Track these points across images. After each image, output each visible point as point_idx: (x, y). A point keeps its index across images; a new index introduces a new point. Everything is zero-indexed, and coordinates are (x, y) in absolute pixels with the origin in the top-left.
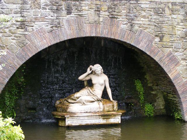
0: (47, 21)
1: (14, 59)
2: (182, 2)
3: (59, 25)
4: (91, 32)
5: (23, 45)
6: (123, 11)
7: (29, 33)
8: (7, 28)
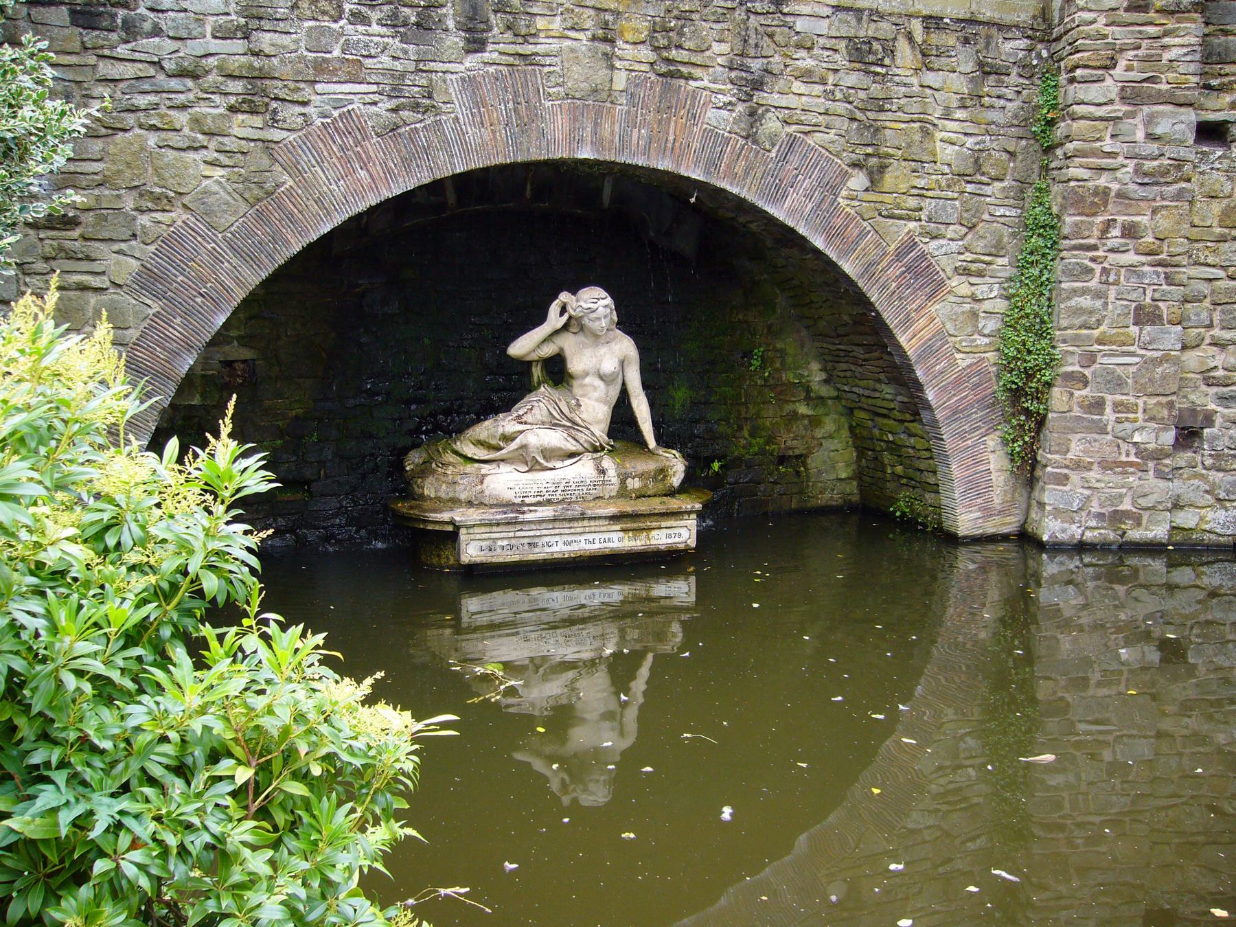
0: (374, 79)
1: (217, 258)
2: (968, 16)
3: (426, 102)
4: (575, 139)
5: (260, 196)
6: (716, 48)
7: (286, 134)
8: (184, 107)
